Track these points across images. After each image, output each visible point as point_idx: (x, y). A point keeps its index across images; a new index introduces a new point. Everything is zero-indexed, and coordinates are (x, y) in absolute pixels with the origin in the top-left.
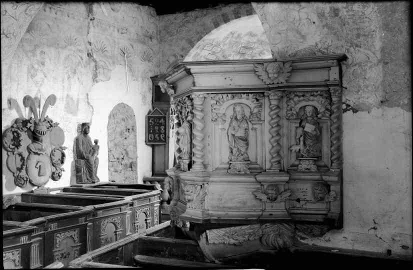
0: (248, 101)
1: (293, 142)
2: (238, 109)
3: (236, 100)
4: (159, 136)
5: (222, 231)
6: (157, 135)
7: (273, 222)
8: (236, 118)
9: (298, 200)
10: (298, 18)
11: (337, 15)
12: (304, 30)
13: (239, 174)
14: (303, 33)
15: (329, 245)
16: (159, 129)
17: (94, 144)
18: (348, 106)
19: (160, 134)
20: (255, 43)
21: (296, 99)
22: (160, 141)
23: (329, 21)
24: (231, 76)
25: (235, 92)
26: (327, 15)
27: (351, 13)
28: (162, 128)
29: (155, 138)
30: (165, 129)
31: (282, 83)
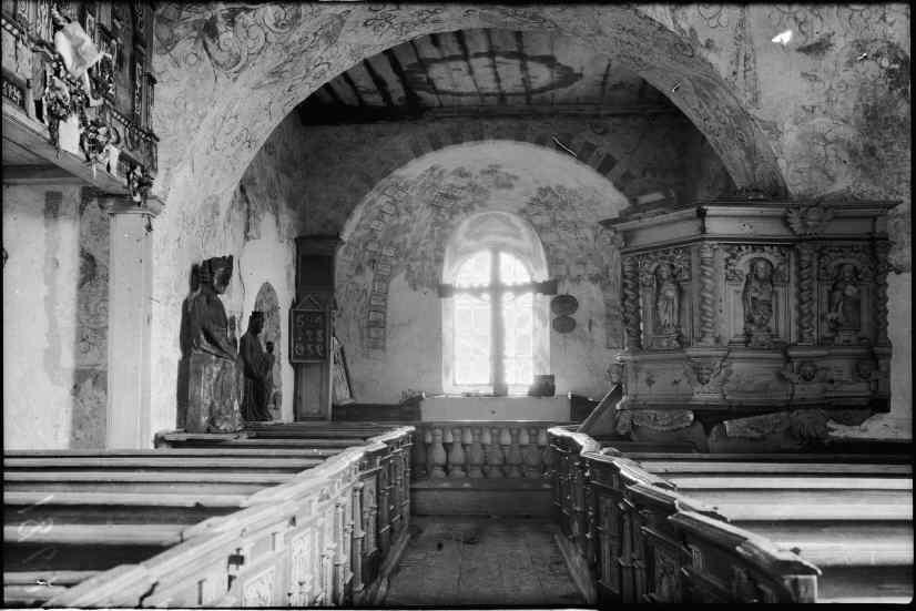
0: (772, 256)
1: (825, 308)
2: (761, 265)
3: (757, 255)
4: (314, 348)
5: (743, 422)
6: (309, 346)
7: (807, 407)
8: (756, 276)
9: (832, 382)
10: (823, 154)
11: (873, 155)
12: (833, 168)
13: (762, 347)
14: (831, 173)
15: (865, 436)
16: (315, 336)
17: (265, 350)
18: (891, 266)
19: (315, 343)
20: (463, 188)
21: (832, 254)
22: (316, 356)
23: (865, 161)
24: (752, 221)
25: (757, 244)
26: (861, 154)
27: (889, 154)
28: (320, 333)
29: (306, 352)
30: (324, 335)
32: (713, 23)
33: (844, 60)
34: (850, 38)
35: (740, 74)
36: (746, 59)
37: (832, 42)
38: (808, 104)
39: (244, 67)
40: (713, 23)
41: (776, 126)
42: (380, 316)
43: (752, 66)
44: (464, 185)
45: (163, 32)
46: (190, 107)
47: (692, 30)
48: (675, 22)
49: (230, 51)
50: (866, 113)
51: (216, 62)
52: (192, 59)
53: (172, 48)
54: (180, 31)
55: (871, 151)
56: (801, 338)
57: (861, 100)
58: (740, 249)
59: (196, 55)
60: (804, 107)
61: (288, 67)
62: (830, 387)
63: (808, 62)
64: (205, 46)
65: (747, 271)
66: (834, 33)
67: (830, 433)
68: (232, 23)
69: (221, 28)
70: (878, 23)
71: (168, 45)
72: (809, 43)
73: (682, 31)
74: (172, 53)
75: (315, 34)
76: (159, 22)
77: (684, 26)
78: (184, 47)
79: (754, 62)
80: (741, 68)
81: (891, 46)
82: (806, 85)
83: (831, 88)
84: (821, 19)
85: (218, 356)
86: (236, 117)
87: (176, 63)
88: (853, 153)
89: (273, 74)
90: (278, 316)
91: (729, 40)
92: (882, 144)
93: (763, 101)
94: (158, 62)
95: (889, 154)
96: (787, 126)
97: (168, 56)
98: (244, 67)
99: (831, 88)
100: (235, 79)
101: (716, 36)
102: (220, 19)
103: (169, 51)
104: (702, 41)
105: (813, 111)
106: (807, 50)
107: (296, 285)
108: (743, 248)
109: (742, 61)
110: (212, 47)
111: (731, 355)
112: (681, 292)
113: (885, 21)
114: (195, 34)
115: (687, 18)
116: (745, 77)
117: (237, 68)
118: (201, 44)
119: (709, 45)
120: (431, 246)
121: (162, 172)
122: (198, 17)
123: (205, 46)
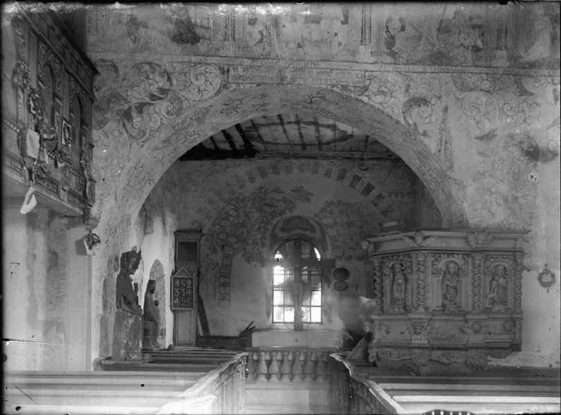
1: (488, 292)
2: (452, 265)
7: (477, 348)
8: (449, 272)
9: (490, 333)
12: (494, 208)
13: (451, 314)
14: (493, 212)
15: (507, 365)
18: (524, 266)
32: (427, 121)
33: (501, 144)
34: (506, 133)
35: (443, 152)
36: (446, 143)
37: (495, 133)
38: (481, 170)
39: (147, 139)
40: (427, 121)
41: (463, 183)
42: (227, 280)
43: (450, 147)
44: (279, 198)
45: (97, 116)
46: (115, 162)
47: (415, 124)
48: (405, 120)
49: (139, 128)
50: (513, 177)
51: (131, 135)
52: (116, 133)
53: (105, 125)
54: (109, 115)
55: (516, 199)
56: (474, 309)
57: (511, 169)
58: (440, 256)
59: (119, 130)
60: (478, 172)
61: (174, 138)
62: (489, 336)
63: (481, 145)
64: (124, 125)
65: (444, 269)
66: (496, 129)
67: (489, 363)
68: (141, 112)
69: (134, 114)
70: (522, 124)
71: (102, 124)
72: (482, 134)
73: (409, 125)
74: (104, 129)
75: (191, 119)
76: (96, 109)
77: (411, 122)
78: (112, 125)
79: (451, 144)
80: (443, 147)
81: (529, 137)
82: (481, 159)
83: (494, 161)
84: (490, 120)
85: (132, 314)
86: (142, 167)
87: (106, 135)
88: (506, 200)
89: (166, 141)
90: (164, 281)
91: (437, 131)
92: (522, 195)
93: (455, 167)
94: (96, 134)
95: (526, 201)
96: (469, 183)
97: (101, 131)
98: (147, 139)
99: (494, 161)
100: (142, 146)
101: (428, 128)
102: (133, 109)
103: (101, 128)
104: (421, 131)
105: (484, 175)
106: (481, 138)
107: (175, 260)
108: (442, 255)
109: (444, 143)
110: (129, 127)
111: (434, 318)
112: (406, 280)
113: (526, 122)
114: (118, 118)
115: (412, 117)
116: (445, 153)
117: (143, 139)
118: (121, 124)
119: (425, 134)
120: (259, 236)
121: (97, 202)
122: (121, 107)
123: (124, 125)
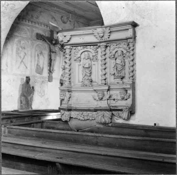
5: (77, 113)
31: (106, 39)
